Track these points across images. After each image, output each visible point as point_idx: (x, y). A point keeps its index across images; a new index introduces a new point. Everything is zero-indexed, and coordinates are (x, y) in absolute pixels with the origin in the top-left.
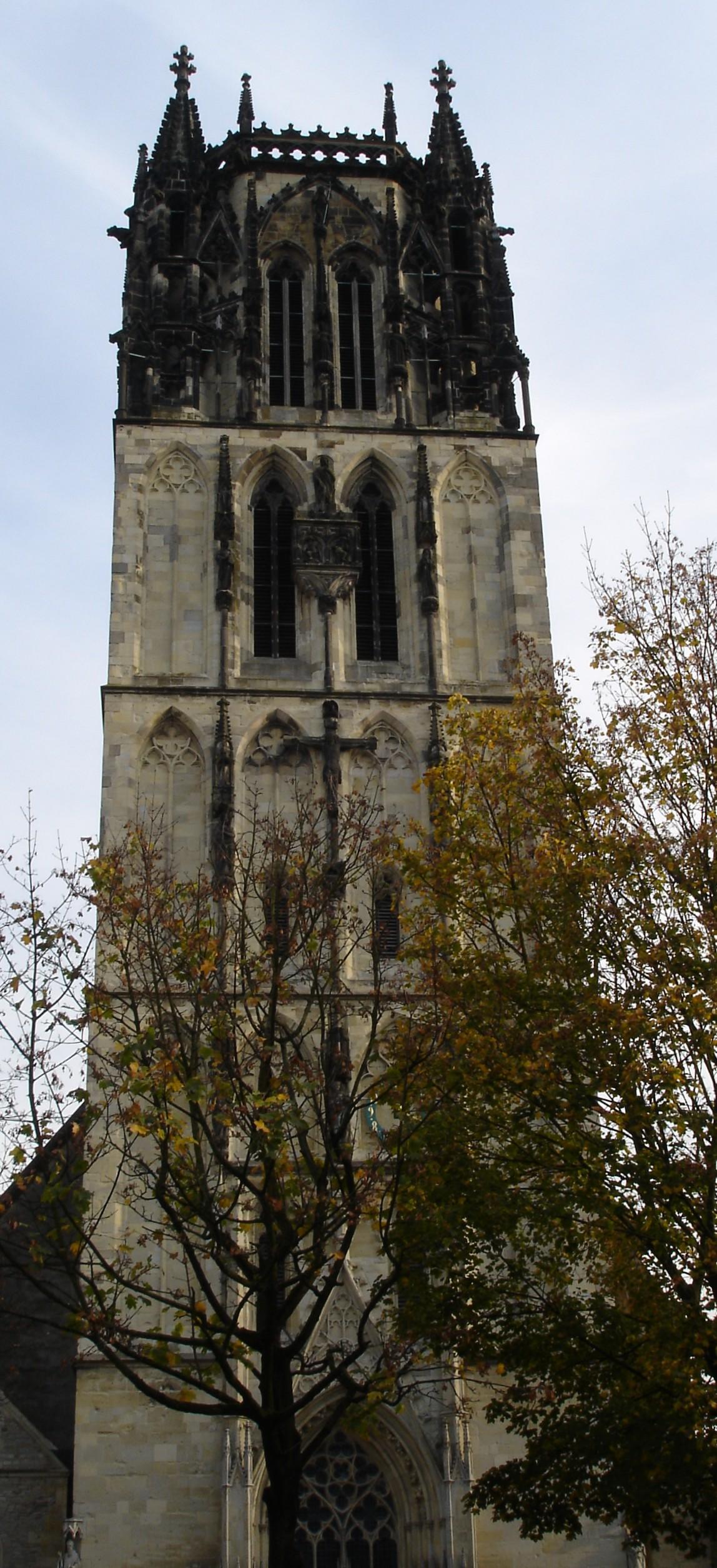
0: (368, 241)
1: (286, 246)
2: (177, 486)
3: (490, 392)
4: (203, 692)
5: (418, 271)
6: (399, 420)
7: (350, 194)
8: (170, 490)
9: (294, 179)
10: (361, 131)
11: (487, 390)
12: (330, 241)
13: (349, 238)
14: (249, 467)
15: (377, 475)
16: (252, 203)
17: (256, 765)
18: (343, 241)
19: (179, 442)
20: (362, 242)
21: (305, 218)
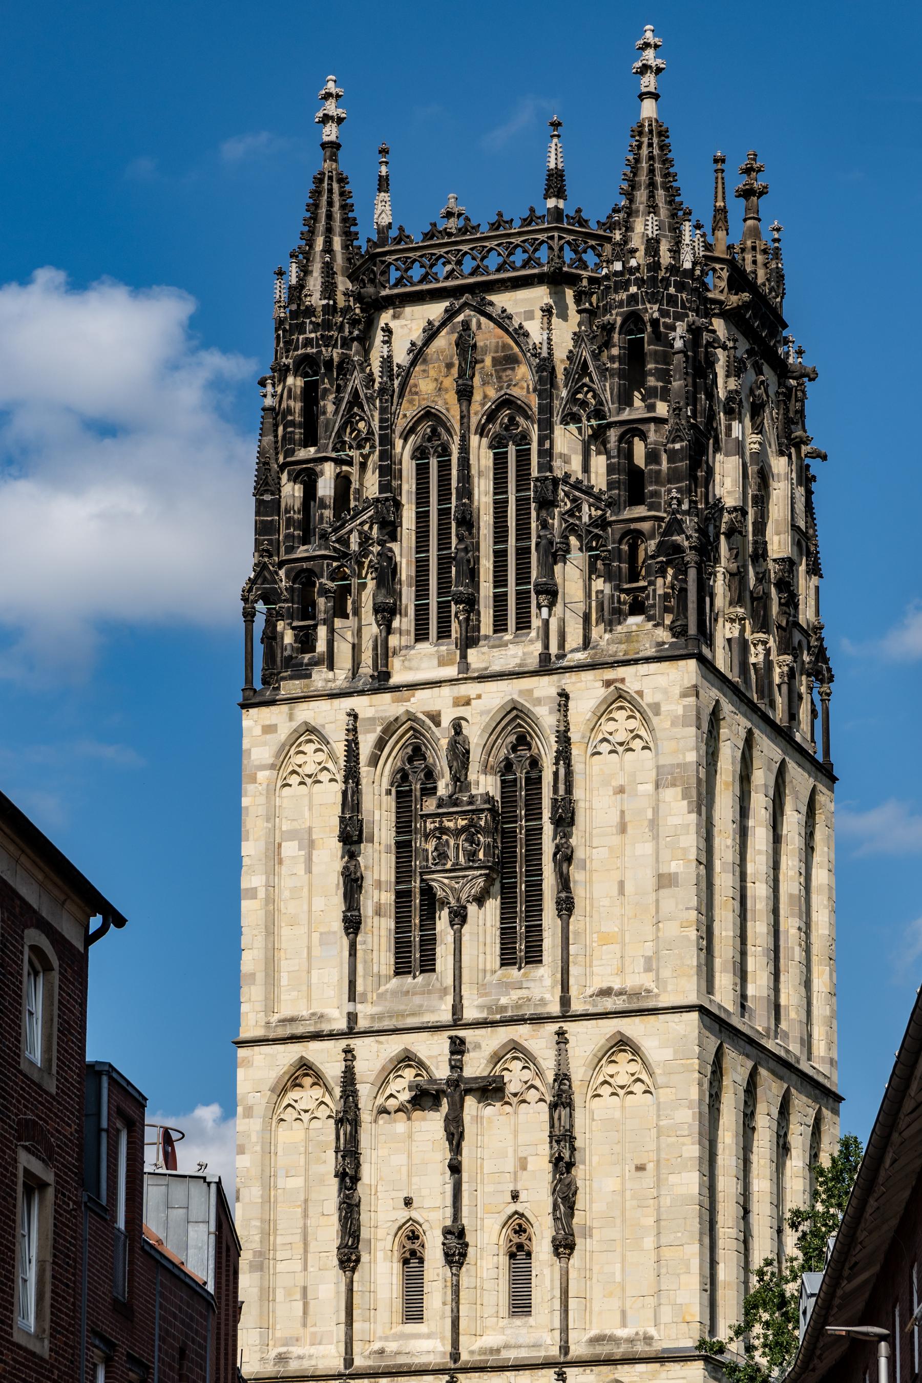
0: (522, 388)
1: (428, 414)
2: (310, 776)
3: (654, 591)
4: (332, 1036)
5: (580, 421)
6: (545, 657)
7: (502, 321)
8: (301, 783)
9: (436, 310)
10: (516, 212)
11: (651, 588)
12: (477, 397)
13: (501, 388)
14: (381, 744)
15: (524, 727)
16: (387, 362)
17: (389, 1113)
18: (492, 393)
19: (306, 723)
20: (516, 392)
21: (449, 366)
